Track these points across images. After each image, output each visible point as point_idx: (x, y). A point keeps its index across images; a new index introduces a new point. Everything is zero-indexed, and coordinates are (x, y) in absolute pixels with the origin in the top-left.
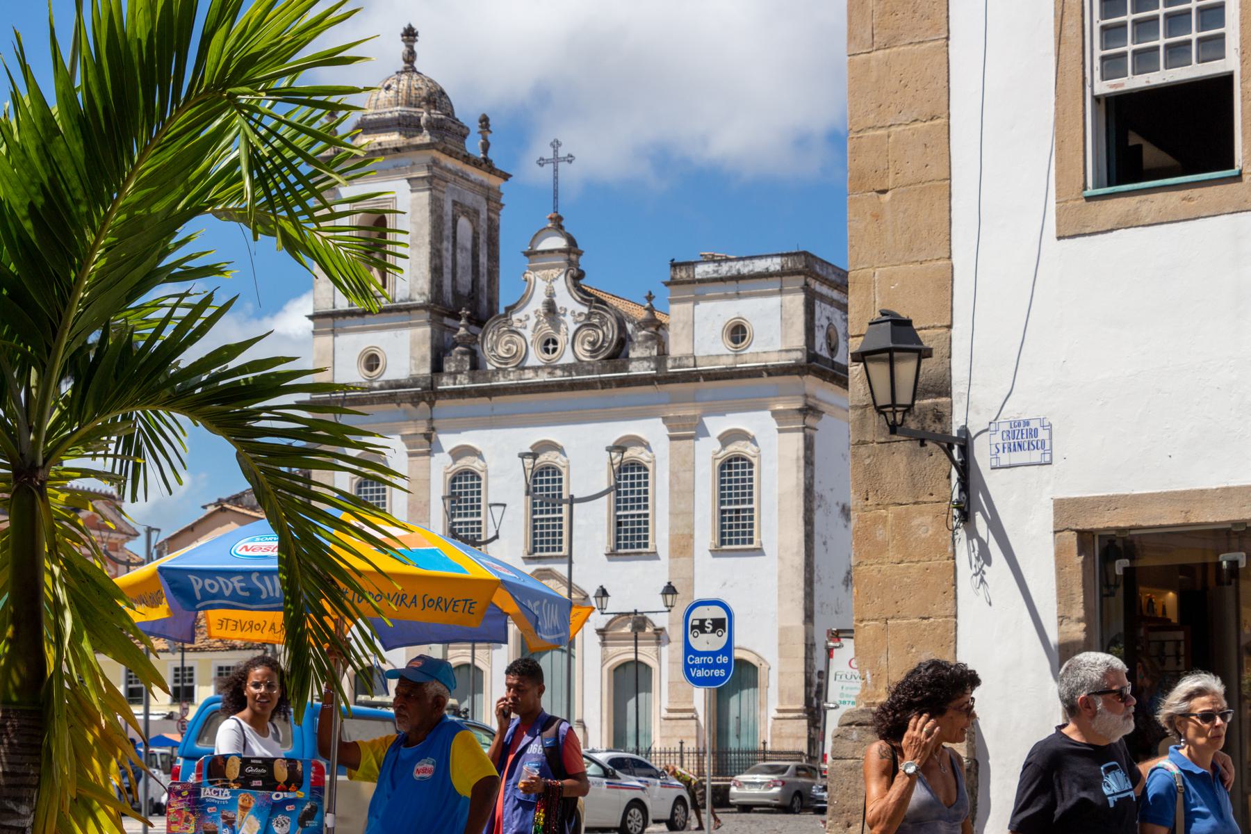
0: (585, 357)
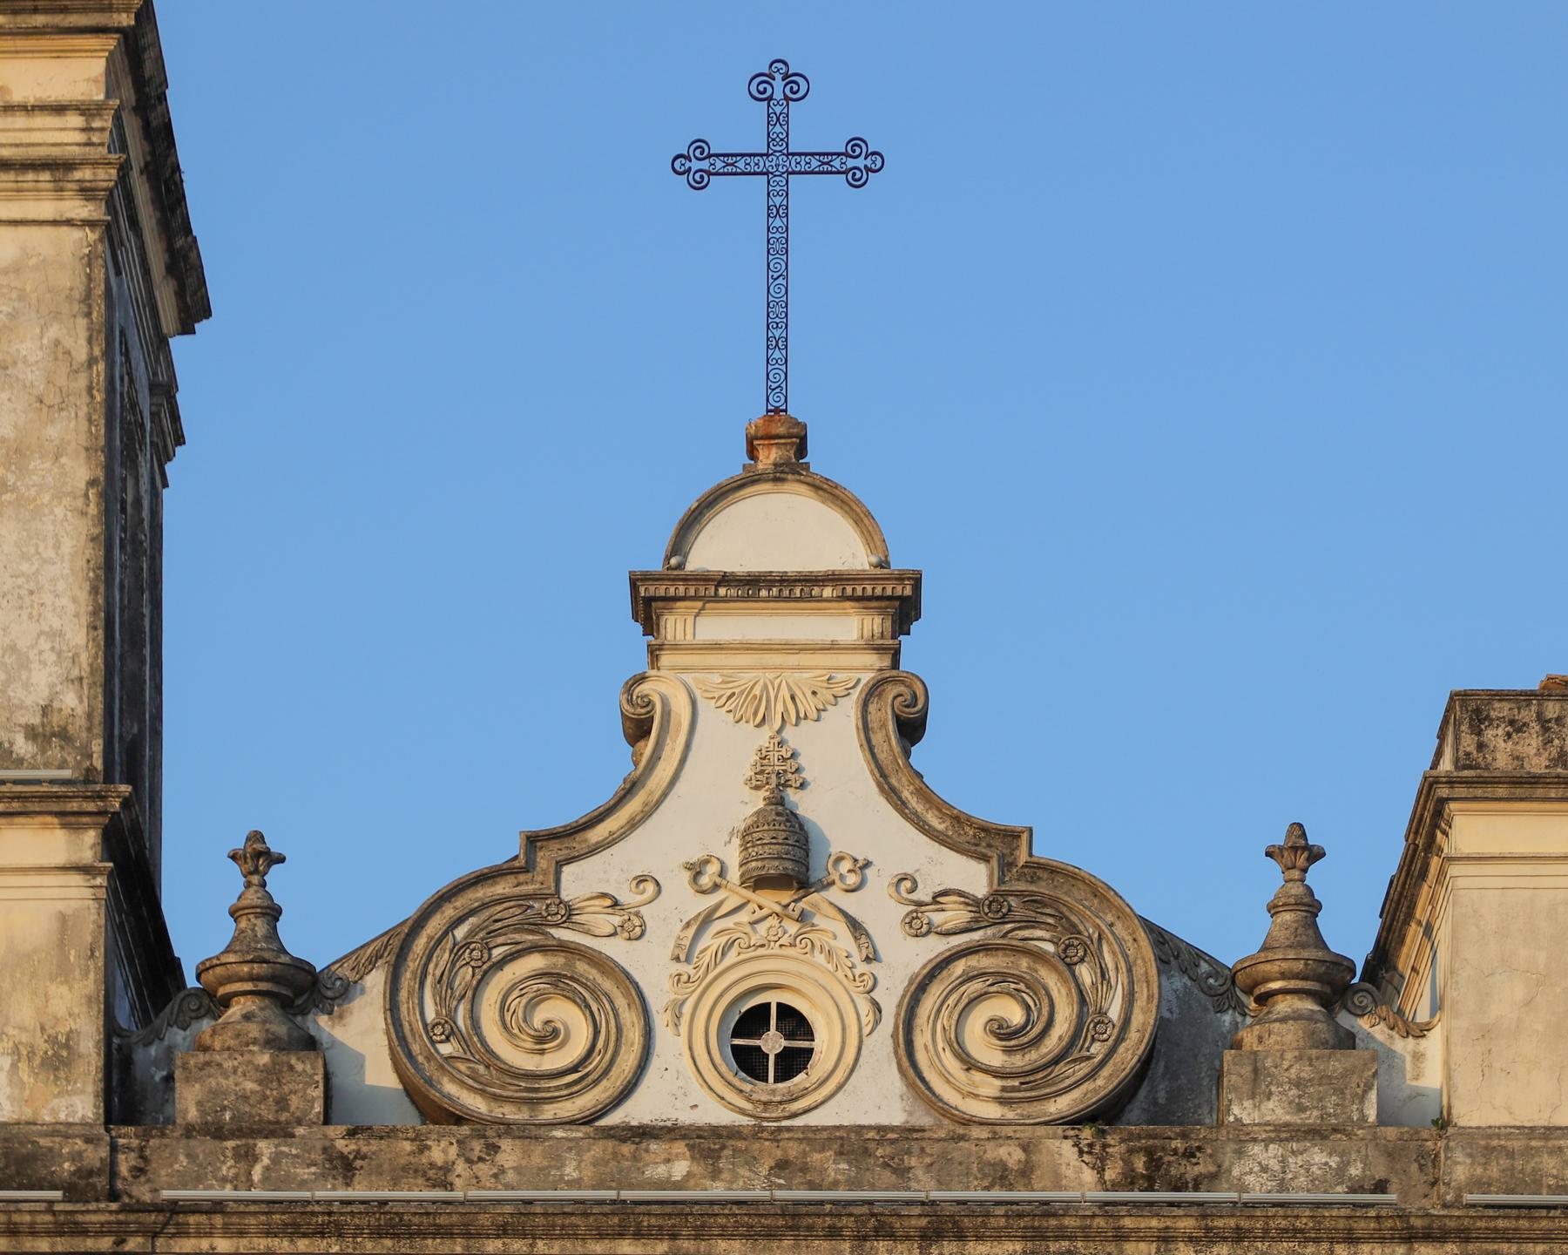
0: (980, 1101)
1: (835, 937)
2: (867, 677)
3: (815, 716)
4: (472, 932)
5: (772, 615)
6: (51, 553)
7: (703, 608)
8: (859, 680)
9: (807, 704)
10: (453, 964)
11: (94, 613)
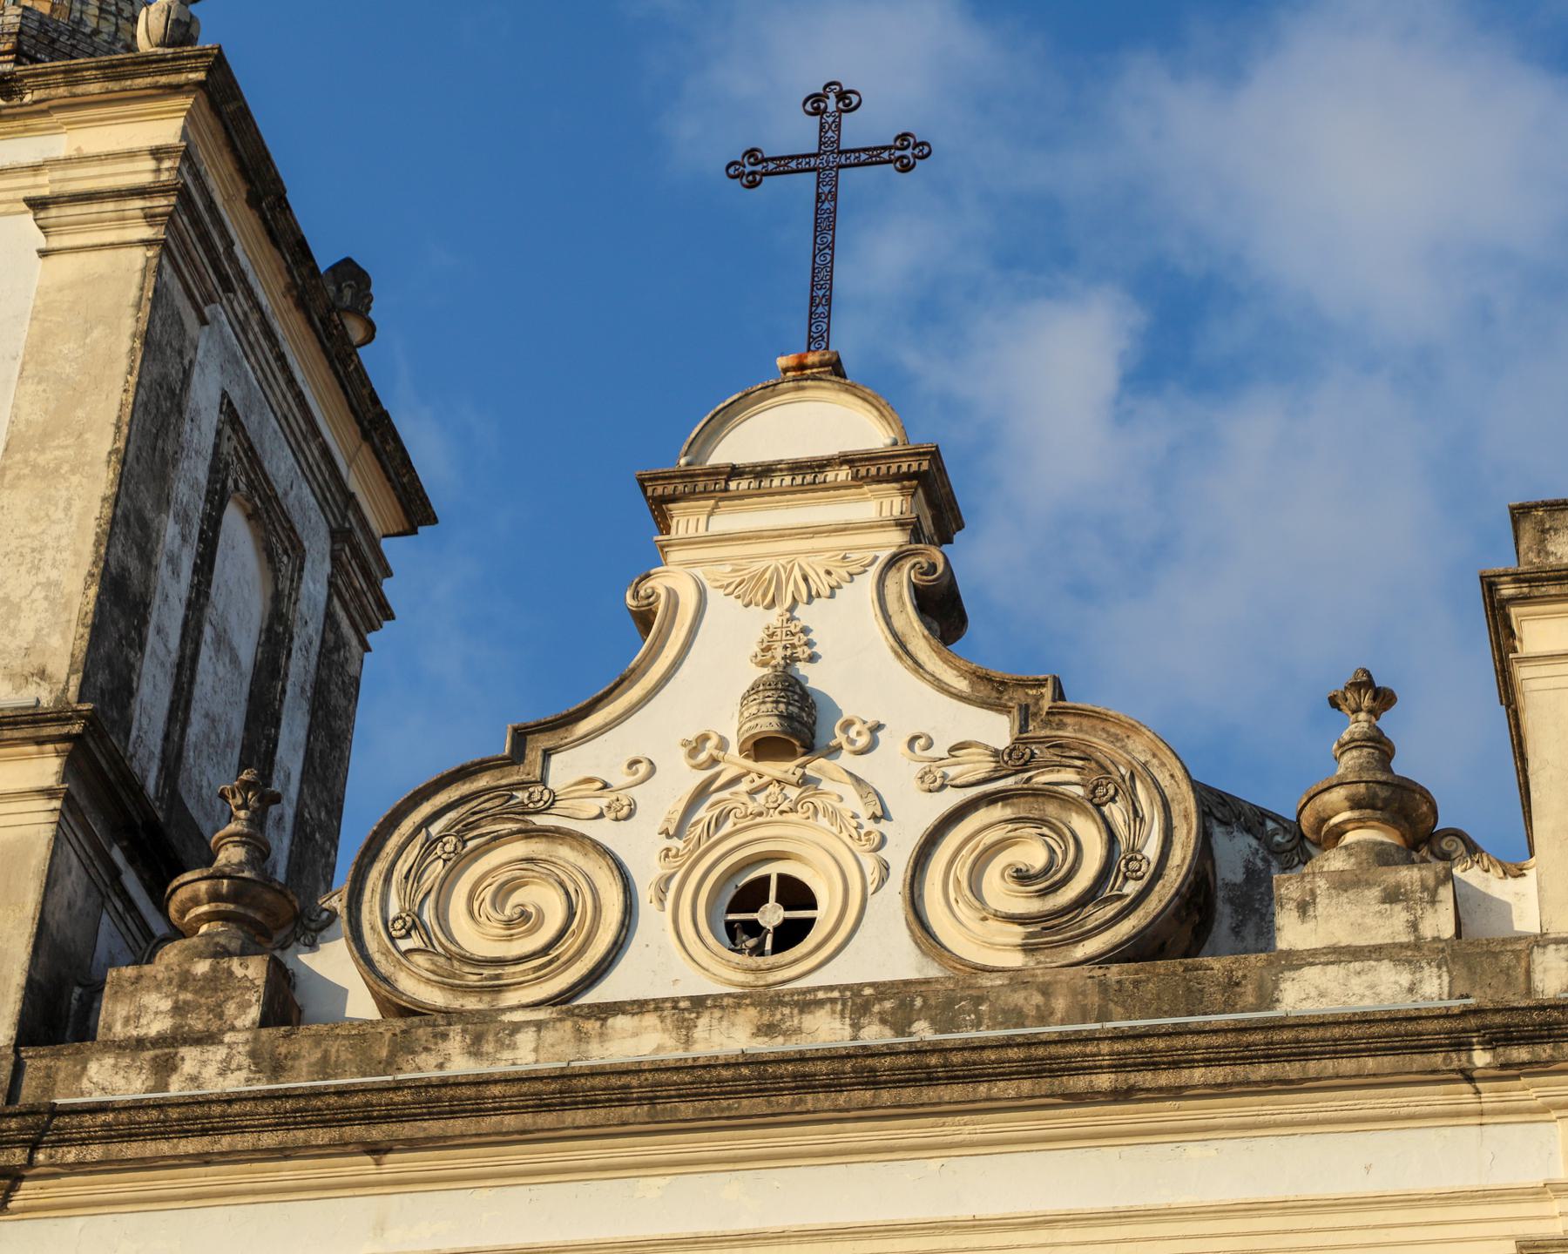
1: (841, 799)
2: (884, 555)
3: (828, 592)
4: (449, 828)
5: (788, 507)
6: (60, 514)
7: (716, 507)
8: (876, 558)
9: (821, 584)
10: (424, 858)
11: (95, 563)
